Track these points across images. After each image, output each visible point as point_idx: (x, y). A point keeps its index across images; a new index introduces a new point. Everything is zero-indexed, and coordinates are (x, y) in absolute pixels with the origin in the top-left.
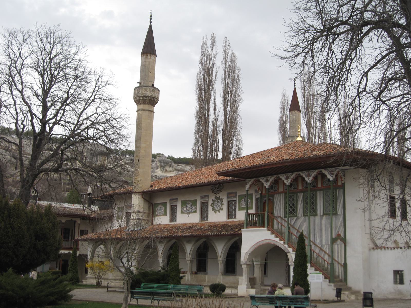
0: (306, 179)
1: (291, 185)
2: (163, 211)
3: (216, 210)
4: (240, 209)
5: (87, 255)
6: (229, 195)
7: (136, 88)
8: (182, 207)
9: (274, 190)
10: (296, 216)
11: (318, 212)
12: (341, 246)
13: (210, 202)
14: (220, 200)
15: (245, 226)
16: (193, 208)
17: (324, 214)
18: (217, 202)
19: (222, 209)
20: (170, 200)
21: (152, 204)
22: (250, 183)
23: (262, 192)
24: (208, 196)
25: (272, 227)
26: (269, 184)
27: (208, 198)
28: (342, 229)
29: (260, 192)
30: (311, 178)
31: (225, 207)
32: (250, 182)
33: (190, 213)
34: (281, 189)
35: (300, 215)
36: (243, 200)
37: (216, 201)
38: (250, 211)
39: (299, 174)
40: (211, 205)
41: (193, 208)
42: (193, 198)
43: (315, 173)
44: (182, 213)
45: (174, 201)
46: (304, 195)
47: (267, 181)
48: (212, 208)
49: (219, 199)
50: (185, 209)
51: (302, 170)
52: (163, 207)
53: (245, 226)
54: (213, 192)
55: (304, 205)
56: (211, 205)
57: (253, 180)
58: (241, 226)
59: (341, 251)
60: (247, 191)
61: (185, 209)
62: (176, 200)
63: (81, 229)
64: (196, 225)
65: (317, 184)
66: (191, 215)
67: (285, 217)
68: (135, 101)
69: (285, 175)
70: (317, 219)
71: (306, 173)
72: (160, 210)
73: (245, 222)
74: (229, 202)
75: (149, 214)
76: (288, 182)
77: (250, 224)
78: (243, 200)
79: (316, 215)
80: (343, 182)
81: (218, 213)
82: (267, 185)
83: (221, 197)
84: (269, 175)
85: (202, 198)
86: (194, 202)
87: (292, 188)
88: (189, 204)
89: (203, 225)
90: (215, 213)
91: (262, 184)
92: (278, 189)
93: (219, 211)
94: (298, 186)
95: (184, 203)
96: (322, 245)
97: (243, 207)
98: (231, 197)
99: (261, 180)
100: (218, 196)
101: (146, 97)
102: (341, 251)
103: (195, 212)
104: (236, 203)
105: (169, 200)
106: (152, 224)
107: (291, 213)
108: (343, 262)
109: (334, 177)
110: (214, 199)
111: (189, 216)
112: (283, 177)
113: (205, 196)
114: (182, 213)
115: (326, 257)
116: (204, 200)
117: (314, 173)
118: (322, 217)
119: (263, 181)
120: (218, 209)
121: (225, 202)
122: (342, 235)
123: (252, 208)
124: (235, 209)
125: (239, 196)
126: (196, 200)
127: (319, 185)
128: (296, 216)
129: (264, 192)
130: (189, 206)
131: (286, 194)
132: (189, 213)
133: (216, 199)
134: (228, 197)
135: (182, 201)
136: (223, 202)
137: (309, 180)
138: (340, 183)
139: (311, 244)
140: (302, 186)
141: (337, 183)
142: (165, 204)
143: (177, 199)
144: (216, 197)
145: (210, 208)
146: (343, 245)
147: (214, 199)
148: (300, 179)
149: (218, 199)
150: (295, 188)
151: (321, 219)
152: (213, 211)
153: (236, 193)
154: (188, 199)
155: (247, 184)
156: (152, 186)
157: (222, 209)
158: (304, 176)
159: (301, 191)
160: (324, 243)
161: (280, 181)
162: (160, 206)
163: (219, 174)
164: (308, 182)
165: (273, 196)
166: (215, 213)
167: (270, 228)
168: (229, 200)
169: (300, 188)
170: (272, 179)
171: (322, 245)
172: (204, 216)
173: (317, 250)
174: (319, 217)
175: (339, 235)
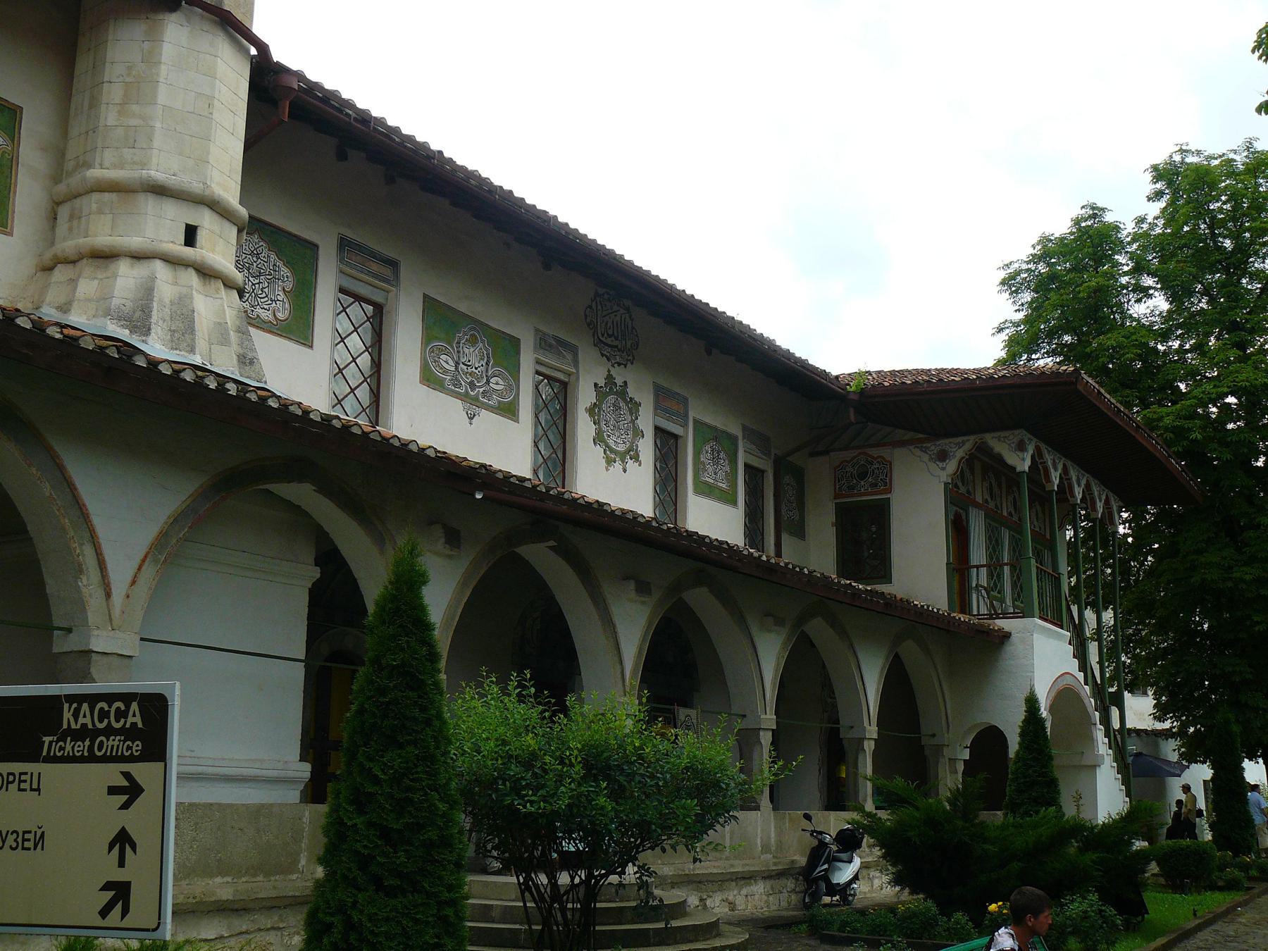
2: (282, 296)
3: (612, 451)
6: (663, 398)
8: (427, 338)
13: (585, 396)
14: (624, 400)
18: (617, 407)
19: (636, 458)
20: (345, 245)
24: (574, 350)
27: (576, 363)
31: (646, 448)
33: (475, 401)
36: (708, 448)
37: (611, 399)
40: (591, 411)
41: (498, 384)
45: (375, 267)
48: (592, 429)
49: (622, 393)
50: (448, 363)
52: (285, 271)
54: (598, 343)
56: (591, 411)
62: (387, 271)
66: (486, 418)
74: (658, 430)
78: (708, 448)
81: (618, 465)
83: (631, 392)
86: (505, 351)
88: (473, 341)
90: (610, 462)
97: (706, 483)
100: (619, 381)
103: (509, 410)
105: (334, 242)
110: (601, 383)
111: (471, 419)
113: (561, 343)
120: (621, 448)
121: (646, 422)
125: (695, 421)
126: (515, 343)
130: (473, 356)
132: (473, 403)
133: (611, 392)
134: (658, 408)
135: (425, 296)
143: (393, 264)
144: (610, 378)
145: (584, 428)
147: (601, 383)
149: (616, 393)
152: (599, 450)
154: (463, 307)
157: (636, 458)
166: (610, 462)
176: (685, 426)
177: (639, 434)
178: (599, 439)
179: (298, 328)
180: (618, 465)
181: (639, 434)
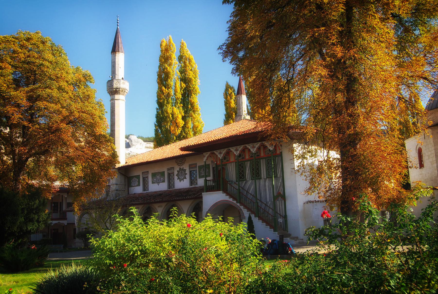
0: (251, 150)
1: (240, 155)
4: (200, 177)
5: (74, 224)
7: (109, 81)
9: (226, 160)
10: (245, 180)
11: (262, 176)
12: (281, 202)
13: (176, 173)
15: (205, 191)
16: (162, 179)
17: (267, 177)
19: (186, 178)
20: (143, 173)
21: (128, 177)
22: (207, 156)
23: (217, 162)
24: (173, 168)
25: (227, 190)
26: (222, 155)
28: (282, 188)
29: (215, 163)
30: (255, 149)
31: (188, 176)
32: (207, 155)
33: (159, 183)
34: (232, 159)
35: (248, 180)
38: (208, 179)
39: (246, 146)
40: (177, 175)
41: (162, 179)
42: (161, 170)
43: (258, 145)
44: (153, 183)
46: (250, 163)
47: (220, 153)
49: (183, 169)
51: (248, 143)
53: (205, 191)
54: (178, 164)
55: (251, 171)
56: (177, 175)
57: (209, 153)
58: (202, 190)
59: (282, 206)
60: (205, 162)
61: (155, 180)
63: (68, 202)
64: (165, 192)
65: (260, 154)
67: (237, 181)
68: (109, 93)
69: (235, 148)
70: (262, 181)
71: (251, 145)
72: (134, 181)
73: (205, 188)
74: (190, 172)
75: (125, 185)
76: (237, 153)
77: (209, 189)
79: (261, 178)
80: (281, 151)
81: (182, 181)
82: (220, 156)
84: (222, 149)
85: (168, 169)
87: (241, 157)
88: (158, 175)
89: (170, 191)
90: (180, 181)
91: (217, 155)
92: (230, 159)
93: (183, 179)
94: (245, 156)
95: (154, 175)
96: (266, 202)
98: (192, 168)
99: (215, 153)
100: (182, 168)
101: (117, 88)
102: (282, 206)
103: (164, 181)
104: (196, 172)
106: (128, 193)
107: (241, 178)
108: (284, 214)
109: (273, 147)
112: (233, 149)
113: (171, 168)
114: (153, 183)
115: (271, 211)
116: (170, 172)
117: (257, 145)
118: (265, 180)
119: (217, 154)
121: (188, 172)
122: (282, 193)
123: (210, 176)
124: (196, 176)
126: (164, 172)
127: (262, 154)
128: (245, 180)
129: (218, 163)
130: (158, 177)
131: (236, 163)
132: (158, 183)
134: (189, 168)
136: (186, 172)
137: (253, 151)
138: (278, 152)
139: (258, 201)
140: (249, 155)
141: (276, 152)
142: (138, 177)
143: (148, 172)
144: (180, 168)
145: (176, 178)
146: (283, 201)
148: (247, 151)
150: (243, 158)
151: (265, 181)
153: (196, 164)
155: (204, 157)
156: (126, 163)
157: (186, 178)
158: (249, 148)
159: (248, 160)
160: (268, 200)
161: (231, 152)
162: (134, 178)
163: (182, 149)
164: (253, 152)
165: (225, 165)
166: (180, 181)
167: (225, 191)
168: (191, 170)
169: (247, 157)
170: (224, 151)
171: (266, 202)
172: (171, 184)
173: (263, 206)
174: (263, 180)
175: (279, 194)
176: (196, 167)
177: (186, 174)
178: (178, 178)
179: (139, 185)
180: (182, 181)
181: (186, 174)
